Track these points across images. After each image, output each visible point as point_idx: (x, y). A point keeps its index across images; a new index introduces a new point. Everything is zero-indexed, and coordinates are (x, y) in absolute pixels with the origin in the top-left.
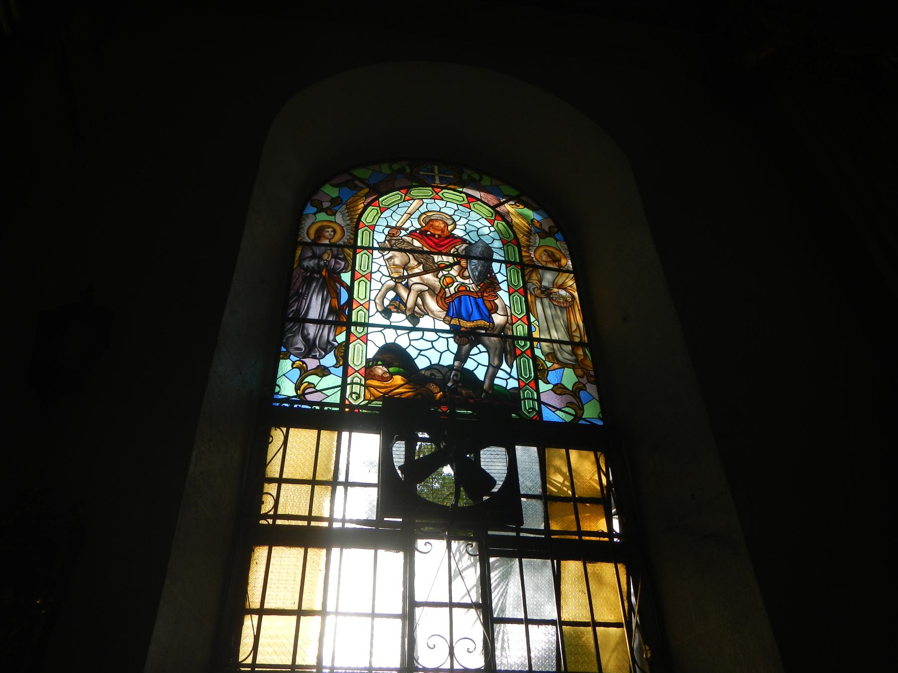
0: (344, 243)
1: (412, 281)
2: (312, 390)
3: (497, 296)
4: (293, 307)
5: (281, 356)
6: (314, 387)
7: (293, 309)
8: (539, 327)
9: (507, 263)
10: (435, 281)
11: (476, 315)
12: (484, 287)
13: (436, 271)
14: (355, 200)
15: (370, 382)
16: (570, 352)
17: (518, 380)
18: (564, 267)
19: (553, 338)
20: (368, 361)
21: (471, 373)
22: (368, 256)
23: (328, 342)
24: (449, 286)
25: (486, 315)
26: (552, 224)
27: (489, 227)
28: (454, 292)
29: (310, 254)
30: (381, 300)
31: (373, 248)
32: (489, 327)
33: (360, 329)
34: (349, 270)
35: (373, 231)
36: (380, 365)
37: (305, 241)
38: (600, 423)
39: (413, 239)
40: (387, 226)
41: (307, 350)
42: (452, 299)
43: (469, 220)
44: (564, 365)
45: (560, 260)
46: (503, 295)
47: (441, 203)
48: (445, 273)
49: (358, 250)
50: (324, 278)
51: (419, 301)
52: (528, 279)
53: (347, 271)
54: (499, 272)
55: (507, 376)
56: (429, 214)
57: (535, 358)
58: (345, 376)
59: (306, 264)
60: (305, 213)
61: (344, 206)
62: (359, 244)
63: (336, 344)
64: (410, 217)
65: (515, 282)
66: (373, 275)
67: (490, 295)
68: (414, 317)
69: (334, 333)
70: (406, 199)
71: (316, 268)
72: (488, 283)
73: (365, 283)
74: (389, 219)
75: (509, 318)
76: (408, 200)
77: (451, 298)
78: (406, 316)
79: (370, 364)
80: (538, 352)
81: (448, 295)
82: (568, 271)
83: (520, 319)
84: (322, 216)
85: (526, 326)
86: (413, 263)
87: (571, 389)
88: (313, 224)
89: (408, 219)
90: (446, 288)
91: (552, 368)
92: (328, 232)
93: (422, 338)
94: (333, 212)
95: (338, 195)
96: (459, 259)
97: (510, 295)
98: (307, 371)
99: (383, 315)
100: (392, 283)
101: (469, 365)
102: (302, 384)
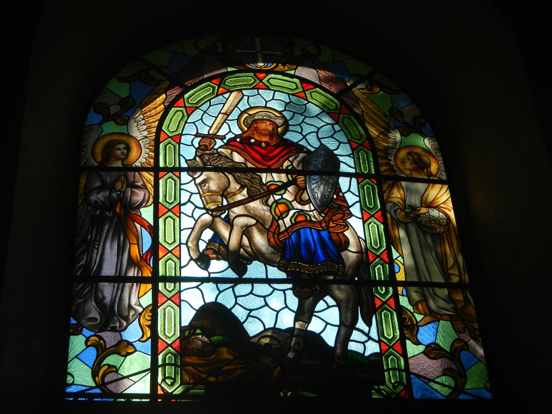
0: (141, 163)
1: (235, 213)
3: (347, 226)
6: (117, 371)
7: (81, 263)
8: (404, 265)
13: (266, 196)
16: (446, 298)
17: (379, 342)
18: (435, 176)
21: (317, 338)
22: (175, 181)
24: (284, 216)
25: (333, 253)
26: (418, 113)
27: (333, 125)
28: (290, 224)
29: (98, 184)
30: (195, 243)
31: (181, 170)
33: (170, 286)
34: (150, 203)
35: (179, 143)
36: (199, 334)
37: (90, 164)
38: (487, 395)
39: (232, 151)
40: (197, 135)
43: (306, 117)
44: (439, 317)
46: (356, 223)
47: (267, 94)
48: (277, 197)
51: (246, 241)
52: (388, 197)
53: (148, 204)
54: (349, 190)
55: (364, 338)
56: (251, 112)
57: (400, 310)
59: (93, 198)
60: (88, 123)
62: (162, 165)
63: (140, 310)
64: (226, 119)
65: (370, 204)
66: (183, 209)
67: (337, 225)
69: (137, 294)
70: (219, 93)
73: (172, 220)
74: (199, 124)
75: (364, 255)
76: (222, 94)
77: (286, 234)
78: (229, 263)
80: (404, 301)
81: (283, 229)
84: (110, 127)
86: (234, 186)
87: (448, 350)
88: (99, 139)
89: (224, 122)
90: (279, 219)
92: (119, 149)
93: (251, 293)
95: (129, 94)
96: (294, 176)
97: (364, 222)
98: (106, 349)
99: (199, 263)
100: (207, 218)
101: (315, 326)
102: (100, 368)
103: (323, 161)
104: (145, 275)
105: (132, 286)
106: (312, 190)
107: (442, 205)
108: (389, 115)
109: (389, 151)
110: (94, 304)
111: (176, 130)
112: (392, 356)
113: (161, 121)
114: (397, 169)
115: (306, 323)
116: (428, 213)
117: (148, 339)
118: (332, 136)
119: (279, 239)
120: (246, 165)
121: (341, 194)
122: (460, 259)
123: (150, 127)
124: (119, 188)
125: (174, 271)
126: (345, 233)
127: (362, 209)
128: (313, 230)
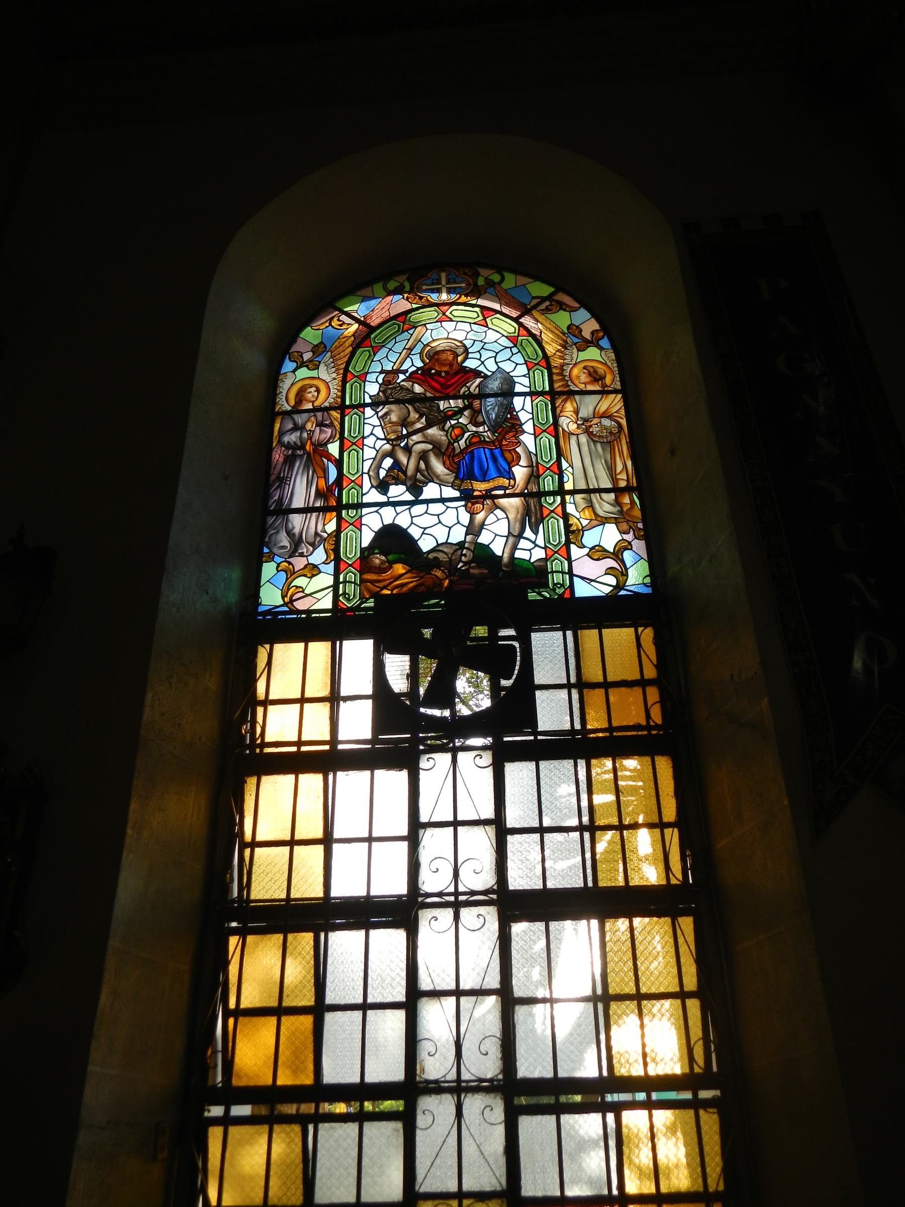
2: (301, 594)
3: (519, 443)
4: (275, 496)
5: (264, 558)
6: (303, 592)
8: (573, 474)
9: (533, 394)
10: (441, 436)
11: (493, 472)
12: (503, 433)
14: (341, 343)
15: (368, 576)
16: (613, 502)
17: (545, 548)
18: (609, 387)
19: (591, 487)
20: (363, 550)
23: (316, 534)
24: (459, 439)
29: (291, 426)
30: (376, 471)
32: (509, 485)
33: (352, 513)
34: (336, 438)
36: (377, 554)
37: (284, 409)
39: (414, 383)
40: (381, 373)
41: (293, 547)
42: (463, 456)
45: (605, 378)
46: (528, 439)
48: (453, 422)
49: (347, 411)
50: (309, 454)
52: (561, 412)
53: (335, 440)
54: (523, 409)
55: (530, 545)
56: (433, 345)
57: (566, 516)
58: (336, 574)
59: (286, 439)
60: (283, 371)
61: (329, 353)
62: (348, 403)
63: (325, 535)
66: (366, 441)
67: (510, 442)
68: (416, 489)
71: (299, 444)
72: (507, 426)
74: (384, 361)
75: (535, 469)
76: (407, 331)
79: (366, 554)
80: (570, 509)
81: (458, 451)
82: (615, 392)
83: (548, 469)
84: (303, 373)
85: (557, 476)
86: (414, 415)
88: (292, 384)
90: (455, 442)
91: (588, 527)
92: (310, 392)
93: (426, 512)
94: (315, 365)
99: (379, 490)
100: (388, 447)
101: (484, 538)
102: (288, 589)
103: (499, 384)
104: (331, 504)
105: (319, 515)
106: (487, 412)
107: (615, 414)
108: (567, 332)
109: (565, 368)
110: (285, 534)
111: (363, 369)
112: (556, 561)
113: (348, 363)
114: (572, 384)
115: (476, 535)
116: (601, 423)
117: (331, 561)
118: (509, 359)
119: (453, 461)
120: (424, 394)
121: (515, 413)
122: (629, 464)
123: (338, 369)
124: (308, 429)
125: (356, 498)
126: (517, 449)
127: (534, 425)
128: (486, 450)
